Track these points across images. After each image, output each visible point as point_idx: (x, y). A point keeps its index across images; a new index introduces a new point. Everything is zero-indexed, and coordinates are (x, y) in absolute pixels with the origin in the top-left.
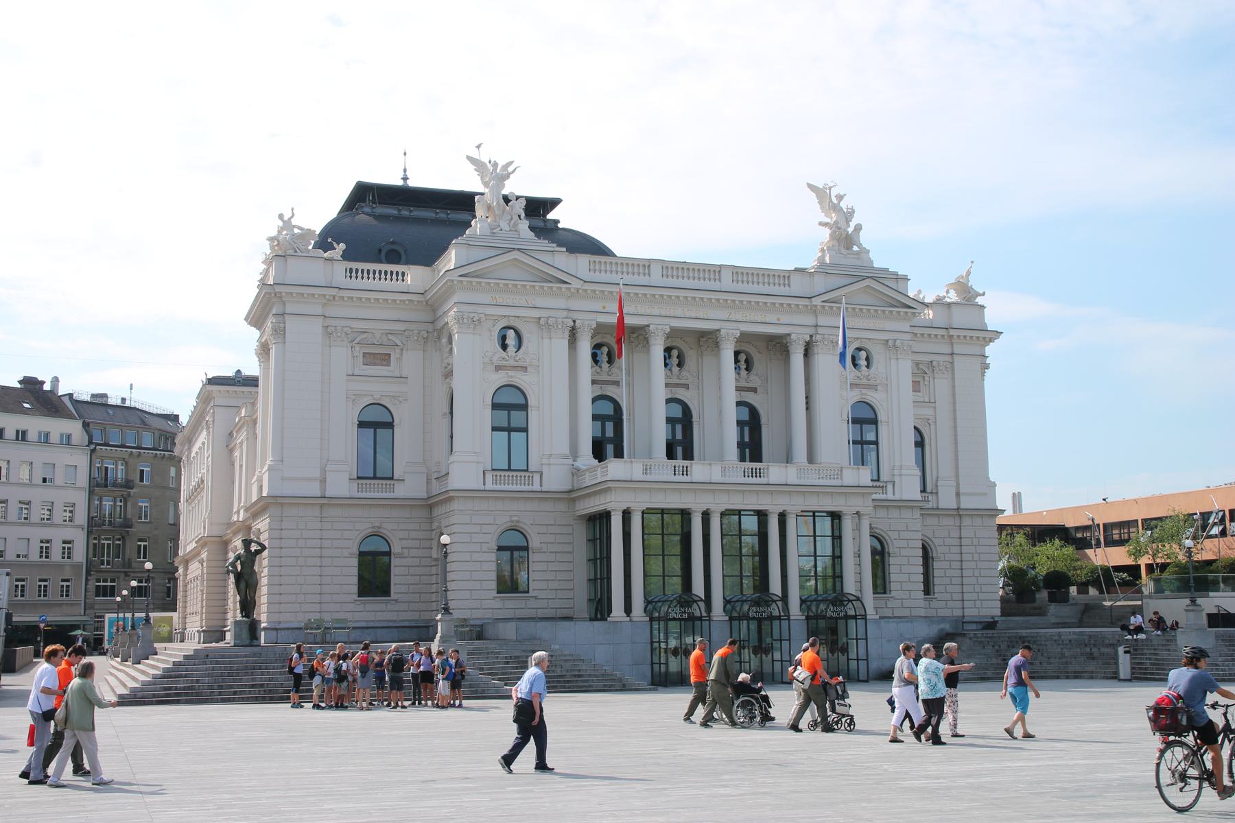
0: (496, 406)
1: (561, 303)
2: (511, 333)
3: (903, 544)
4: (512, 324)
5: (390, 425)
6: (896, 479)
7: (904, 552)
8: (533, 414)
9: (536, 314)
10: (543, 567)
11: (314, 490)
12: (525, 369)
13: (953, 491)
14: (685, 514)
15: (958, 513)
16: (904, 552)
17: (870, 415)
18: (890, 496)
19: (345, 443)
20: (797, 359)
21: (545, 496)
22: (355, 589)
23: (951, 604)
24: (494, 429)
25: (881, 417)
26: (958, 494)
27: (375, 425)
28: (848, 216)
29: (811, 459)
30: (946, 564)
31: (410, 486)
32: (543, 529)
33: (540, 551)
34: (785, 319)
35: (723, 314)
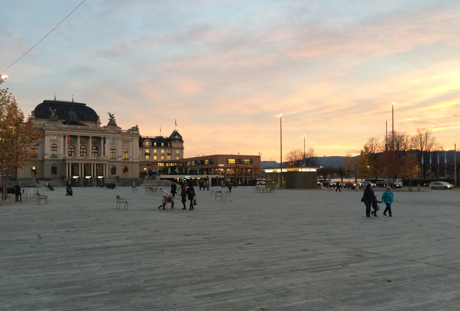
1: (62, 132)
14: (78, 164)
15: (133, 163)
20: (102, 141)
21: (59, 160)
28: (113, 118)
29: (104, 155)
31: (40, 158)
35: (89, 134)
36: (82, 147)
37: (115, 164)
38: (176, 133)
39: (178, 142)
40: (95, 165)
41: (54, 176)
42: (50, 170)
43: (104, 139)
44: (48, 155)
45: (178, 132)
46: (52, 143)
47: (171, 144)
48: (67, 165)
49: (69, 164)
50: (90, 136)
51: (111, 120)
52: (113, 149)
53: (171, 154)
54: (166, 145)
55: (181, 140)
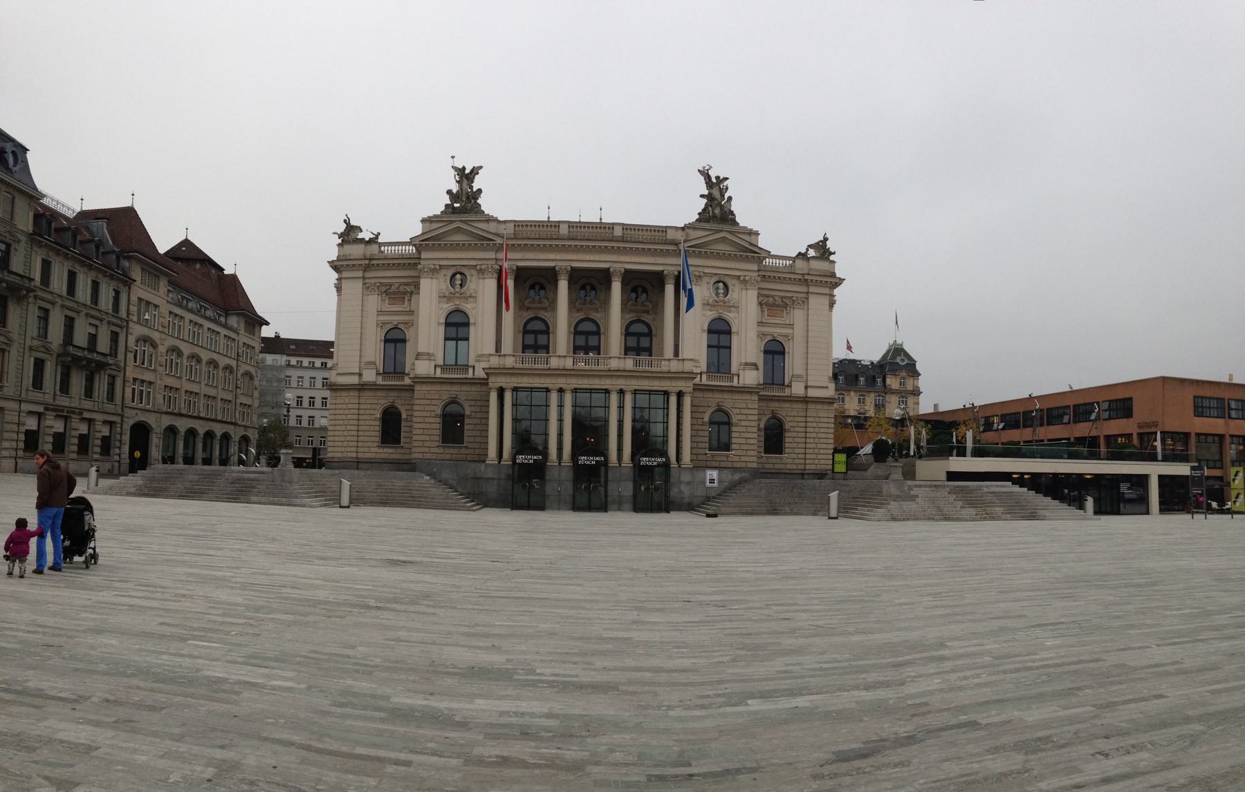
0: (447, 324)
2: (458, 276)
3: (744, 417)
4: (459, 269)
5: (404, 341)
6: (741, 373)
7: (743, 423)
8: (472, 328)
9: (474, 263)
10: (472, 427)
11: (354, 380)
12: (466, 298)
13: (803, 385)
15: (806, 400)
16: (743, 423)
17: (726, 328)
18: (735, 383)
19: (374, 350)
20: (670, 289)
22: (377, 439)
23: (797, 461)
24: (446, 339)
25: (734, 329)
26: (806, 387)
27: (396, 341)
30: (795, 434)
32: (473, 403)
33: (470, 417)
34: (660, 260)
35: (614, 258)
36: (582, 328)
37: (728, 401)
38: (897, 350)
39: (904, 374)
40: (628, 399)
41: (451, 452)
42: (436, 425)
43: (678, 282)
44: (429, 356)
45: (905, 347)
46: (448, 307)
47: (884, 381)
48: (494, 397)
49: (501, 391)
50: (614, 267)
51: (709, 197)
52: (719, 332)
53: (883, 406)
54: (871, 381)
55: (911, 369)
